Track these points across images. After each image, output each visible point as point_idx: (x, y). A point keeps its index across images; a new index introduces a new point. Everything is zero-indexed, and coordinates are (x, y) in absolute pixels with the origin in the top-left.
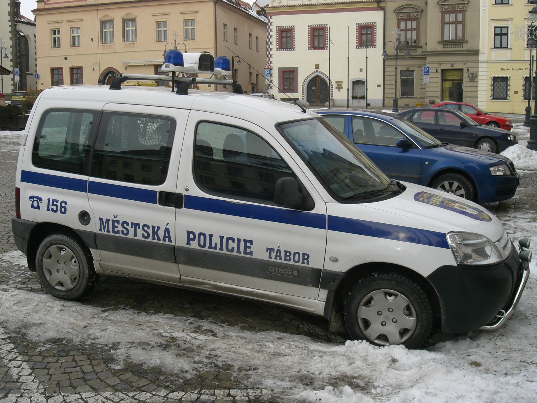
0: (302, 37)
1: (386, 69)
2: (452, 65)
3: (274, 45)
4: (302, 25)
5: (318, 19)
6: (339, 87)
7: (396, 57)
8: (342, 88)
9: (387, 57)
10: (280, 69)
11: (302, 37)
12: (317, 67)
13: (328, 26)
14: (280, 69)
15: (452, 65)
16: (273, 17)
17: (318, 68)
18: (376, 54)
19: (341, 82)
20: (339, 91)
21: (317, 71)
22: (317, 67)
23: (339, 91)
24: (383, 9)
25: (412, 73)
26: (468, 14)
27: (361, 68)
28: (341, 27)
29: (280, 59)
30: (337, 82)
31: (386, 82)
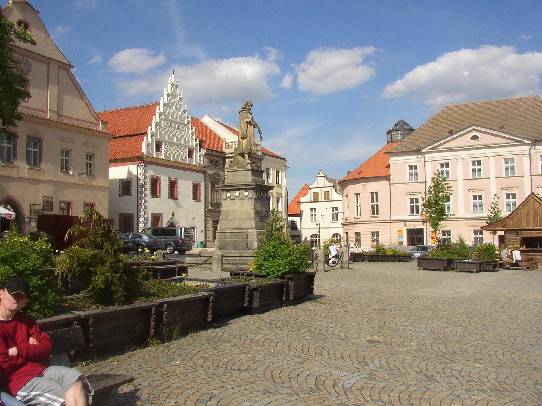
0: (164, 187)
3: (148, 192)
5: (174, 174)
11: (164, 187)
12: (173, 214)
22: (173, 214)
24: (204, 172)
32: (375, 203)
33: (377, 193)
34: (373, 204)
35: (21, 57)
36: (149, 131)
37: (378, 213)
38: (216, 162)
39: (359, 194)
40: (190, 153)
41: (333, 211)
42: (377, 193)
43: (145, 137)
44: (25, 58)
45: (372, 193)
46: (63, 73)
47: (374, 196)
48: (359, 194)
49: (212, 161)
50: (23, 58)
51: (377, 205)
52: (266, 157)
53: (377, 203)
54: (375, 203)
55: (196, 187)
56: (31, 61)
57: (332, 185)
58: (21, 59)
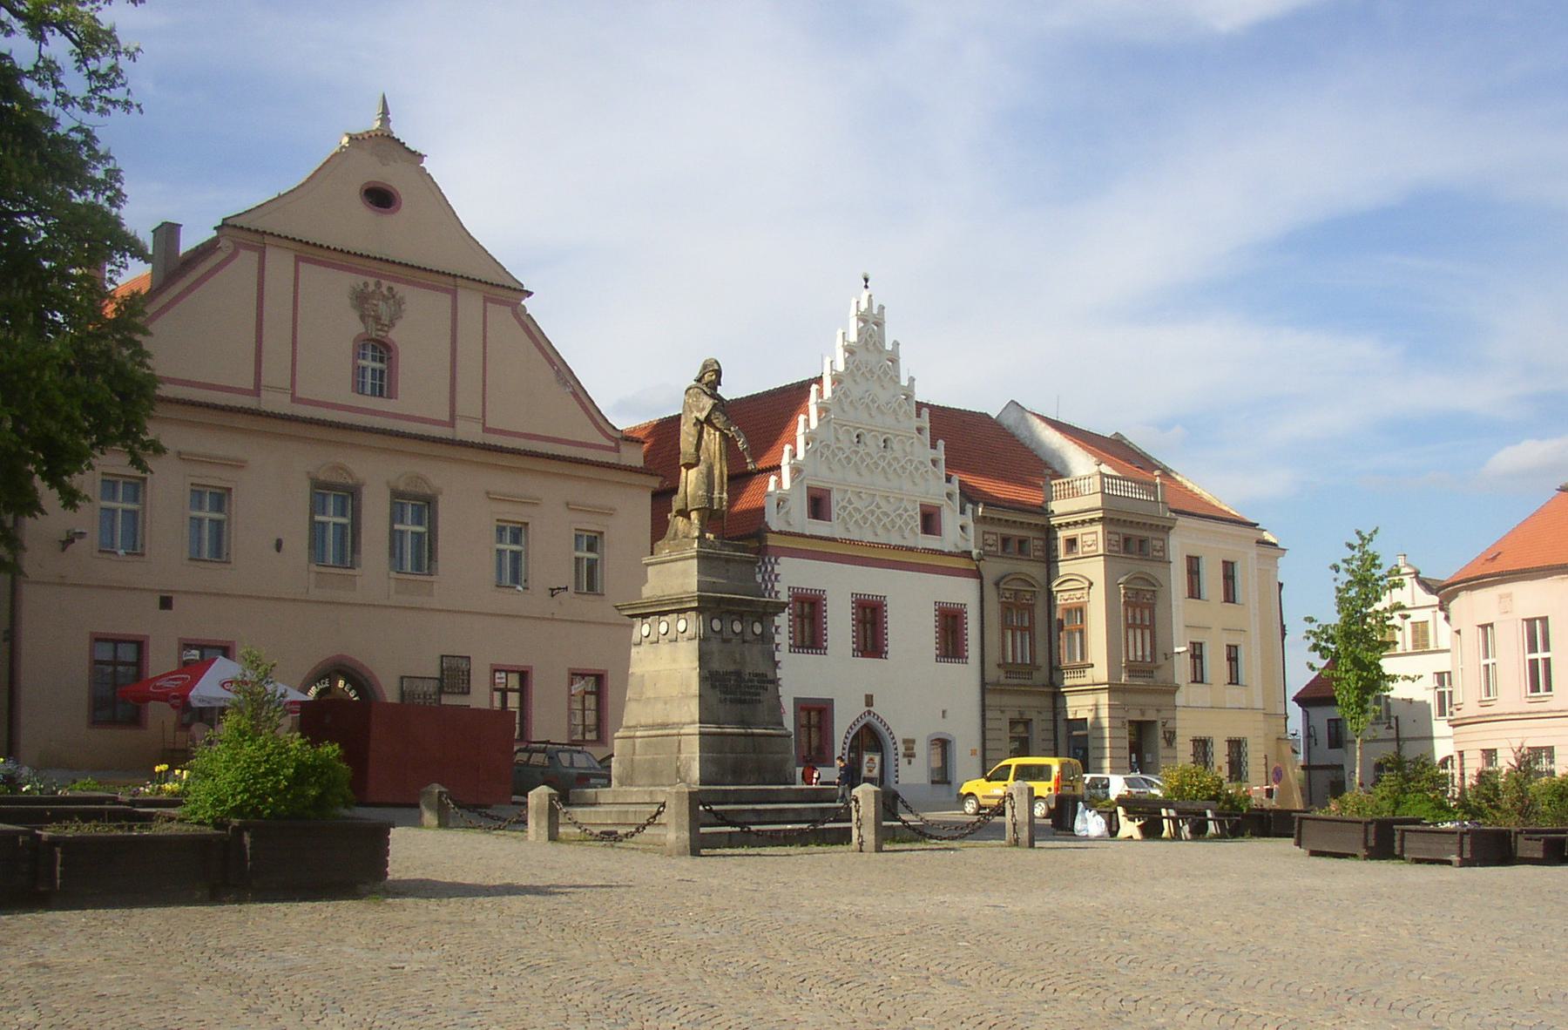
0: (840, 624)
1: (989, 714)
2: (1143, 713)
4: (841, 588)
5: (871, 581)
6: (910, 755)
8: (913, 756)
9: (985, 688)
11: (840, 624)
12: (869, 700)
15: (1143, 713)
16: (782, 560)
18: (964, 678)
19: (913, 741)
22: (869, 700)
24: (977, 574)
25: (1027, 723)
26: (1158, 611)
28: (912, 603)
30: (905, 741)
31: (989, 745)
32: (1540, 655)
33: (1544, 620)
34: (1533, 656)
35: (372, 281)
36: (785, 460)
37: (1549, 688)
38: (1022, 542)
39: (1491, 625)
40: (930, 521)
41: (1441, 683)
42: (1544, 620)
43: (773, 479)
44: (385, 284)
45: (1530, 622)
46: (500, 316)
47: (1537, 632)
48: (1491, 625)
50: (378, 285)
51: (1547, 661)
52: (1182, 521)
53: (1546, 655)
54: (1540, 655)
55: (950, 622)
56: (400, 289)
57: (1435, 599)
58: (372, 288)
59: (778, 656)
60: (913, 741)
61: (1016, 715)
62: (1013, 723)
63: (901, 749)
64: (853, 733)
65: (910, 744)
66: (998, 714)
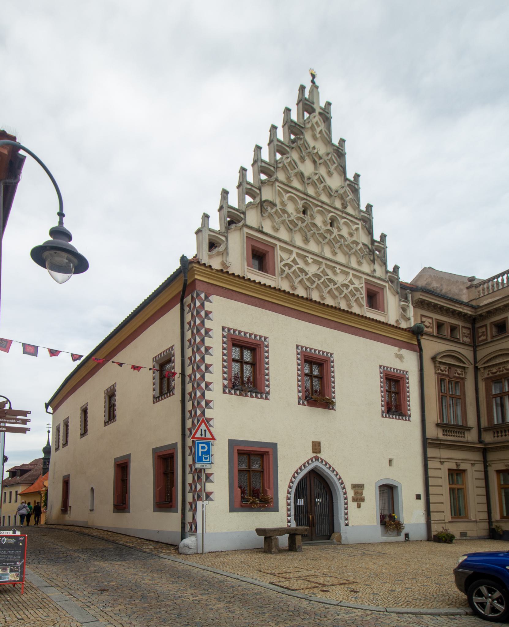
0: (283, 373)
4: (285, 339)
6: (359, 499)
7: (438, 444)
8: (363, 500)
10: (232, 443)
11: (283, 373)
12: (316, 447)
13: (335, 357)
14: (232, 443)
17: (319, 452)
19: (362, 486)
20: (359, 506)
21: (317, 459)
22: (316, 447)
23: (359, 506)
27: (391, 457)
28: (359, 365)
29: (232, 419)
31: (431, 490)
49: (440, 325)
59: (208, 395)
60: (362, 486)
61: (454, 466)
62: (451, 472)
63: (351, 493)
64: (297, 481)
65: (358, 488)
66: (437, 465)
